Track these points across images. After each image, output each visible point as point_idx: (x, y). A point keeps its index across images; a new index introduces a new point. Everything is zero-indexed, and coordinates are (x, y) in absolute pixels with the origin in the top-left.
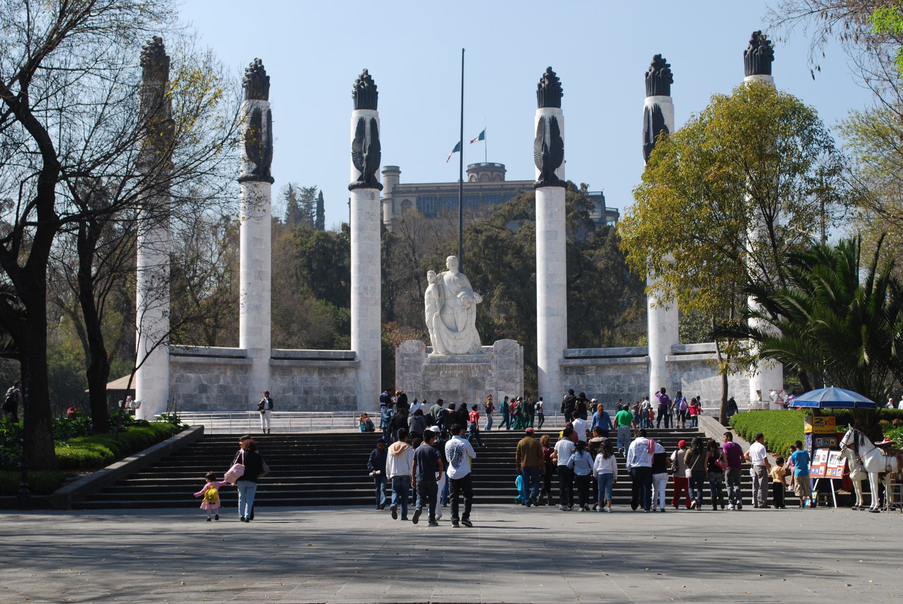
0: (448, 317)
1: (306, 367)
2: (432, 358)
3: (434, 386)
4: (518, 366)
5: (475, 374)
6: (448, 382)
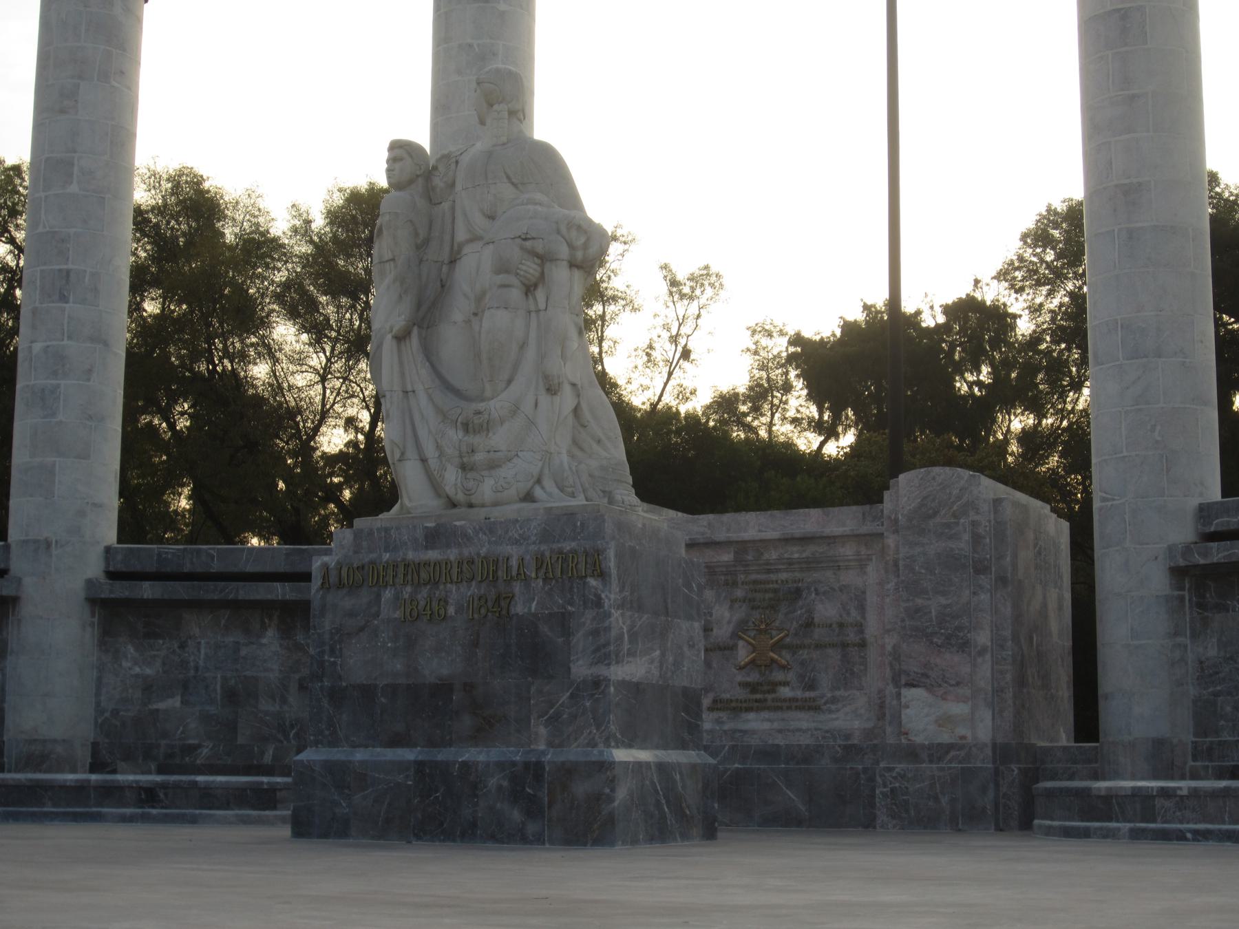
0: (452, 340)
1: (236, 606)
4: (984, 580)
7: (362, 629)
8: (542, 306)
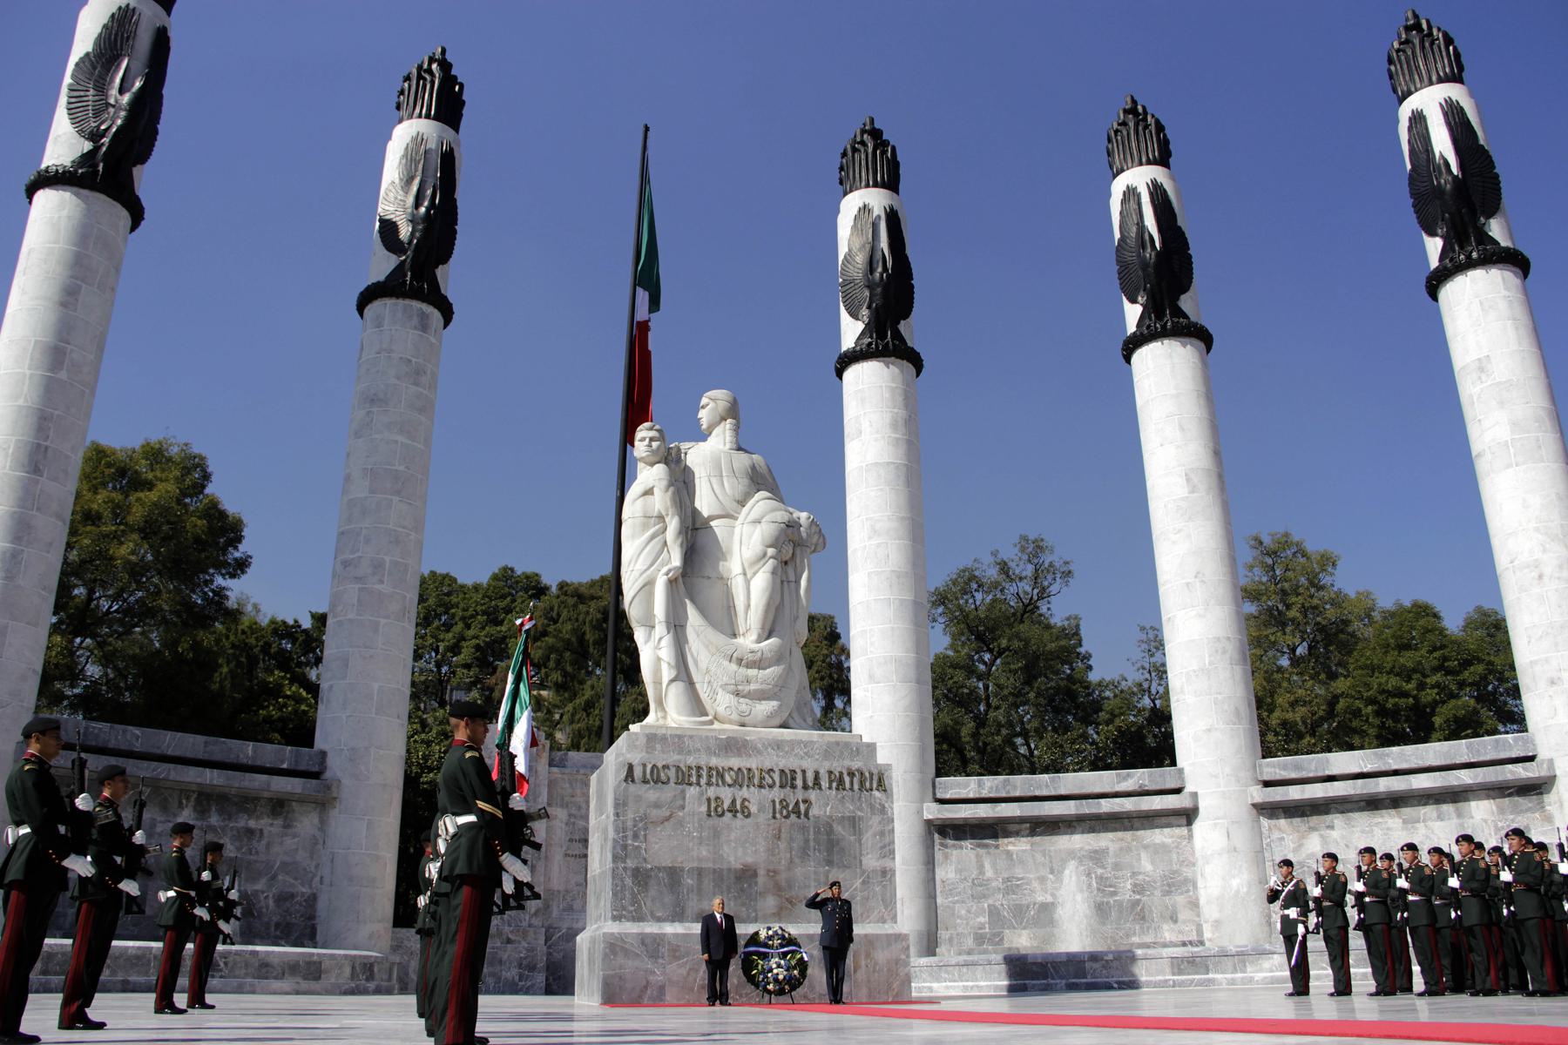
2: (652, 739)
3: (662, 849)
5: (824, 805)
6: (716, 834)
7: (668, 819)
8: (792, 578)
